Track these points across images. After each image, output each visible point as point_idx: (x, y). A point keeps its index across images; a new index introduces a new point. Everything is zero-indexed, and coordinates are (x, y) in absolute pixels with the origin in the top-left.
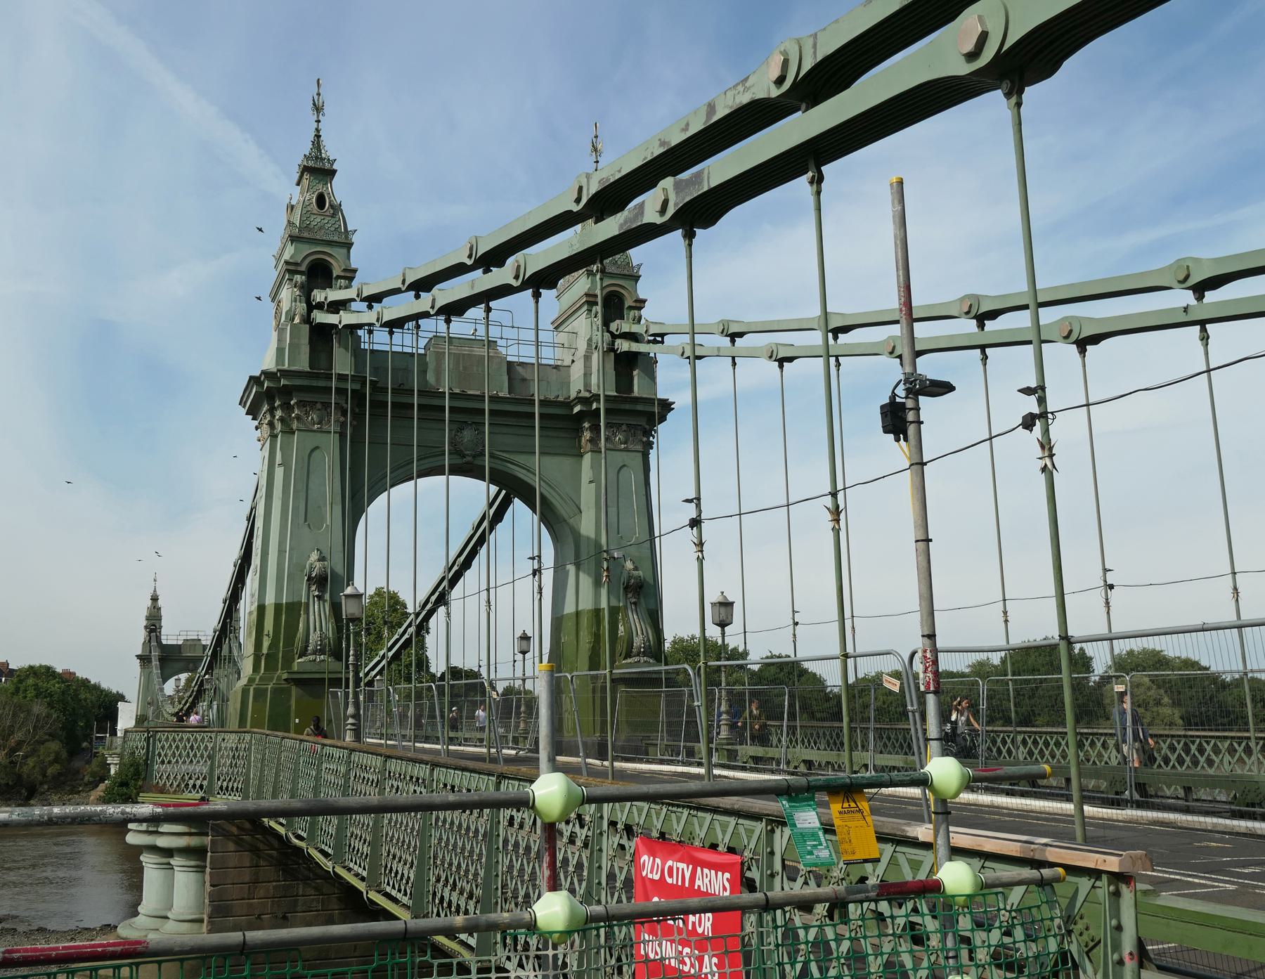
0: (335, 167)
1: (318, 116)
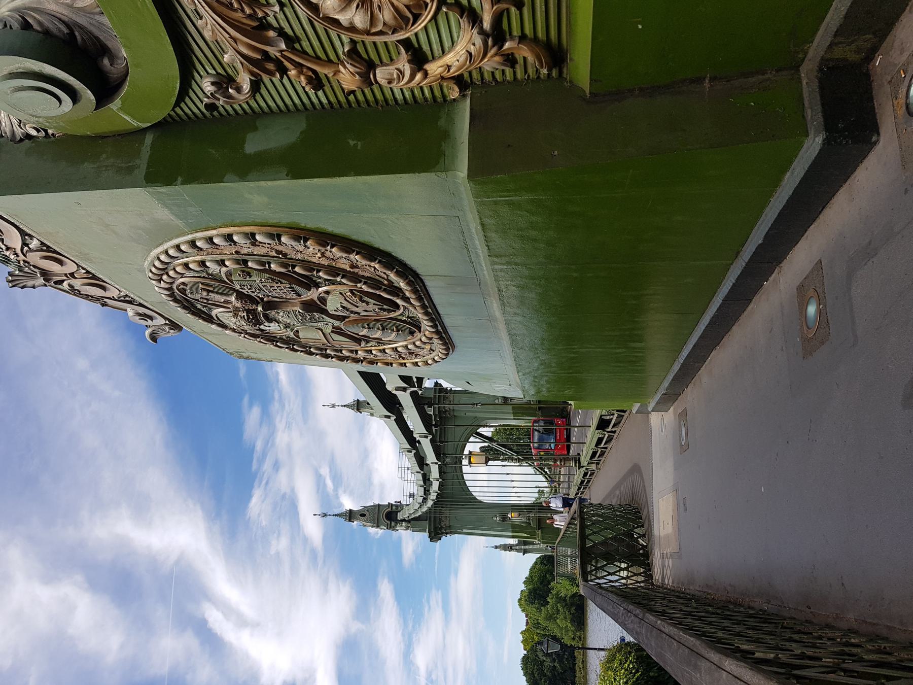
0: (348, 509)
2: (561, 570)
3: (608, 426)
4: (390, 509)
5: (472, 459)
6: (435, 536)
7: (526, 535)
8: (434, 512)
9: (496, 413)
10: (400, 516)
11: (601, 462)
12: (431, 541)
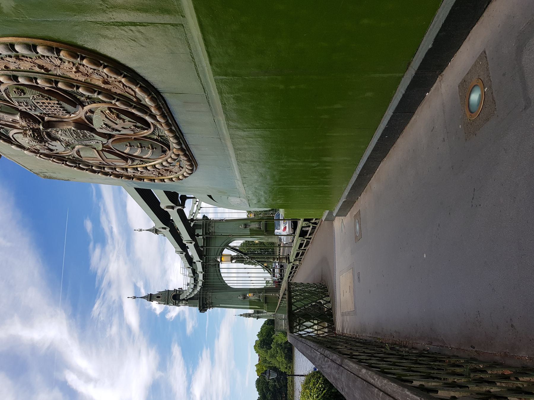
0: (149, 294)
2: (279, 328)
3: (307, 235)
4: (175, 293)
6: (203, 308)
7: (258, 307)
8: (202, 294)
11: (302, 259)
12: (200, 312)
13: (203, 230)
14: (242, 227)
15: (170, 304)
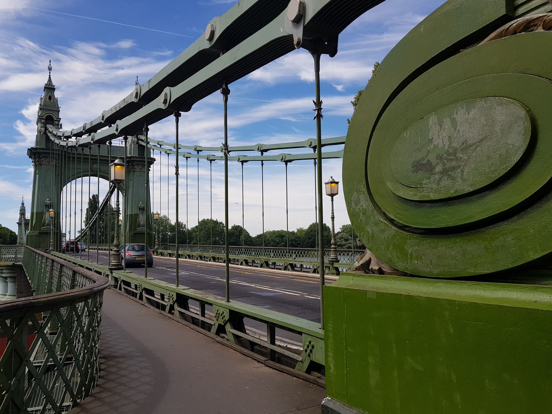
0: (55, 88)
1: (50, 71)
3: (181, 307)
4: (55, 119)
5: (118, 166)
6: (32, 153)
7: (34, 223)
9: (132, 202)
10: (50, 128)
11: (118, 290)
12: (28, 149)
13: (137, 157)
14: (141, 204)
15: (41, 112)
